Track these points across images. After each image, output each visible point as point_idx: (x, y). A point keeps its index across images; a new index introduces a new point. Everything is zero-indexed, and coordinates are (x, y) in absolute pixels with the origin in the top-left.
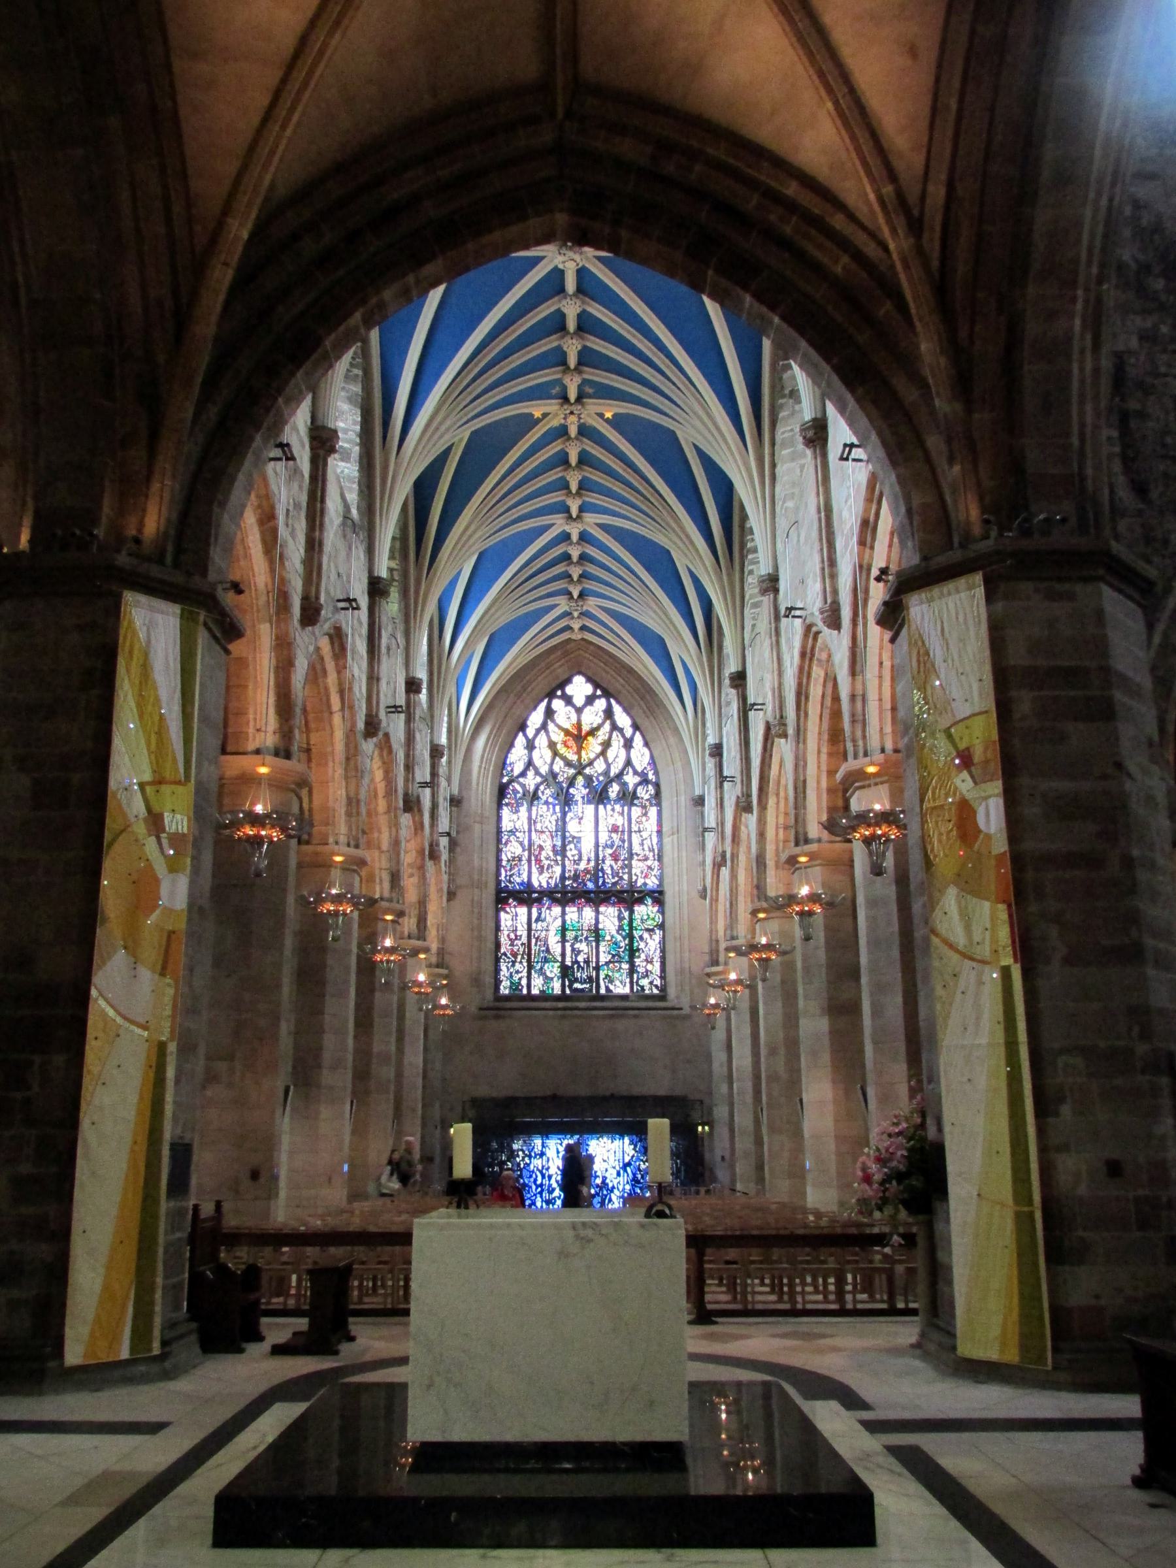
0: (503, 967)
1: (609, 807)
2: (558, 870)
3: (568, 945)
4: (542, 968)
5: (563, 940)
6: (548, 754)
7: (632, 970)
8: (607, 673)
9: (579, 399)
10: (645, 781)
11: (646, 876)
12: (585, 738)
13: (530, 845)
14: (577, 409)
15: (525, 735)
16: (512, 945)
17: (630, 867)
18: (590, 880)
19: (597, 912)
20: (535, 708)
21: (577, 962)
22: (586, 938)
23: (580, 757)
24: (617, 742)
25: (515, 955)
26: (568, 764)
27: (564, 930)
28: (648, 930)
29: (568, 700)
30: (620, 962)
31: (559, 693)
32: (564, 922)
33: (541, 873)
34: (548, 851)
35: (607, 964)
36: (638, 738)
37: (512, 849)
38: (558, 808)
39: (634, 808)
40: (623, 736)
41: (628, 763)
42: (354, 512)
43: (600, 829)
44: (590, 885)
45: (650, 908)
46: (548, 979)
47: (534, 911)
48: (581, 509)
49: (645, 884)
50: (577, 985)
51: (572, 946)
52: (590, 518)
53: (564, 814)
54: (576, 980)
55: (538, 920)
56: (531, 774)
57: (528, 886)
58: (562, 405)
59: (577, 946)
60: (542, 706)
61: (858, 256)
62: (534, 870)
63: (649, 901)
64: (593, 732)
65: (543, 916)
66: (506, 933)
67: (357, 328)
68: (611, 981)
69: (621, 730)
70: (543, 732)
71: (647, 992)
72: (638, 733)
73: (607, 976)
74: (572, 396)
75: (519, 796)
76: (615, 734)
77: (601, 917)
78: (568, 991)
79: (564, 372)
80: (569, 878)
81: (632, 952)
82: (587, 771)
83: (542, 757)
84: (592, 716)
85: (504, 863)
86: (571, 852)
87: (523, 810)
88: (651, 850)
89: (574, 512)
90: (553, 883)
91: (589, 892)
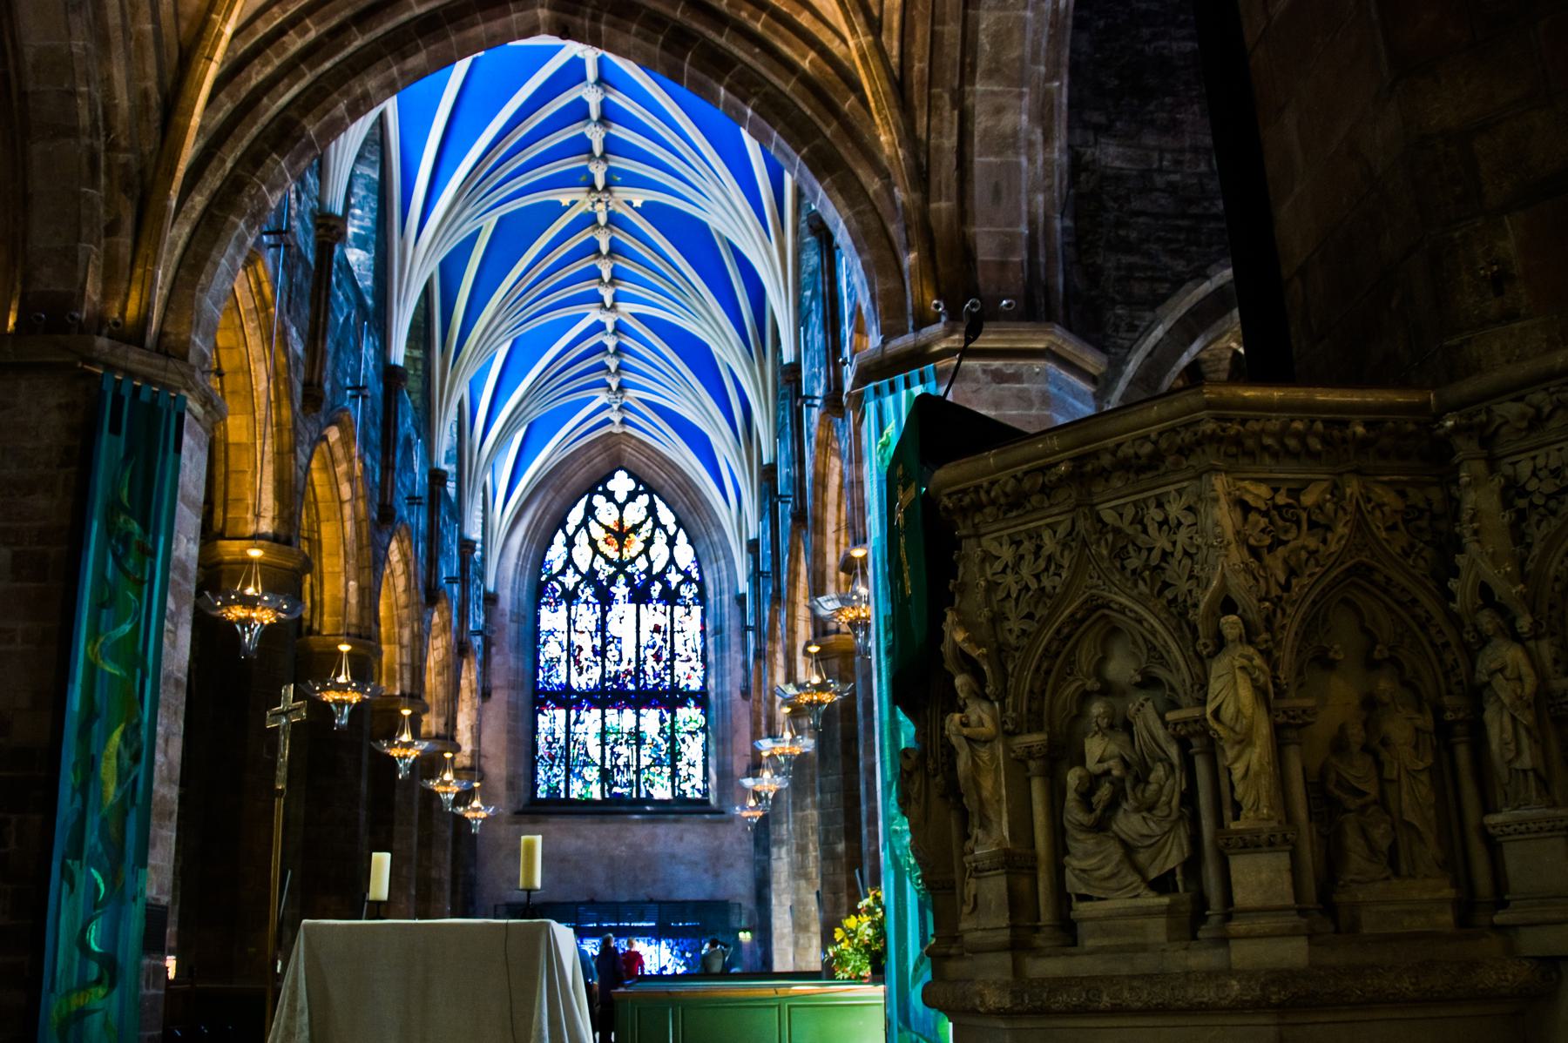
0: (541, 771)
1: (650, 606)
2: (597, 672)
3: (607, 748)
5: (603, 743)
6: (590, 551)
7: (674, 773)
8: (650, 467)
9: (607, 188)
10: (687, 578)
11: (689, 678)
12: (627, 535)
13: (570, 644)
14: (605, 197)
15: (565, 532)
16: (550, 748)
17: (672, 667)
18: (631, 681)
19: (638, 715)
21: (617, 766)
22: (627, 741)
23: (621, 555)
24: (660, 539)
25: (553, 758)
26: (609, 561)
27: (604, 733)
28: (690, 733)
29: (610, 496)
30: (662, 766)
31: (600, 489)
32: (604, 723)
33: (580, 674)
34: (587, 653)
35: (648, 767)
36: (681, 533)
37: (551, 650)
38: (598, 607)
39: (677, 608)
40: (666, 532)
41: (672, 560)
42: (370, 302)
44: (631, 687)
45: (693, 709)
46: (586, 783)
47: (573, 713)
48: (616, 298)
49: (688, 686)
50: (616, 790)
52: (625, 307)
53: (604, 613)
54: (616, 784)
55: (576, 722)
56: (570, 572)
57: (567, 687)
58: (589, 193)
59: (617, 749)
60: (582, 503)
61: (824, 52)
63: (692, 703)
64: (635, 529)
65: (581, 719)
66: (543, 735)
67: (343, 118)
69: (664, 528)
70: (583, 529)
71: (689, 796)
72: (681, 531)
73: (648, 779)
74: (600, 183)
75: (557, 594)
76: (657, 530)
78: (607, 796)
79: (589, 160)
80: (609, 679)
81: (675, 755)
82: (629, 569)
83: (582, 555)
84: (635, 513)
85: (542, 664)
86: (612, 653)
87: (563, 608)
89: (608, 302)
90: (592, 685)
91: (631, 692)
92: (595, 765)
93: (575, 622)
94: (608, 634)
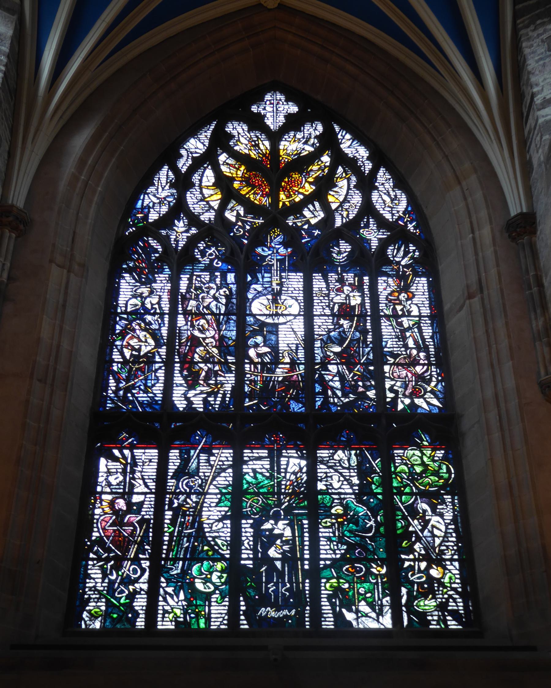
0: (95, 573)
1: (332, 277)
3: (247, 526)
4: (185, 572)
11: (415, 394)
17: (380, 377)
18: (296, 399)
20: (193, 133)
22: (288, 511)
23: (276, 199)
28: (424, 495)
30: (367, 561)
32: (238, 476)
35: (336, 564)
38: (231, 277)
39: (381, 280)
43: (317, 310)
44: (296, 407)
45: (428, 452)
47: (174, 454)
49: (413, 406)
51: (256, 526)
54: (265, 601)
56: (180, 225)
60: (206, 135)
62: (178, 379)
68: (349, 604)
73: (337, 590)
76: (340, 170)
77: (322, 469)
88: (422, 347)
92: (222, 558)
93: (185, 299)
94: (250, 319)
